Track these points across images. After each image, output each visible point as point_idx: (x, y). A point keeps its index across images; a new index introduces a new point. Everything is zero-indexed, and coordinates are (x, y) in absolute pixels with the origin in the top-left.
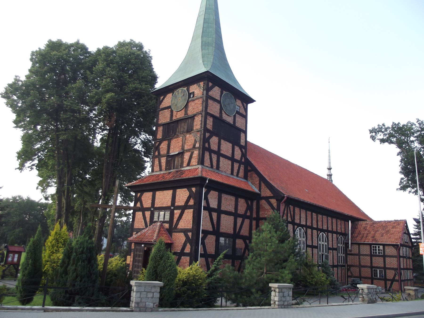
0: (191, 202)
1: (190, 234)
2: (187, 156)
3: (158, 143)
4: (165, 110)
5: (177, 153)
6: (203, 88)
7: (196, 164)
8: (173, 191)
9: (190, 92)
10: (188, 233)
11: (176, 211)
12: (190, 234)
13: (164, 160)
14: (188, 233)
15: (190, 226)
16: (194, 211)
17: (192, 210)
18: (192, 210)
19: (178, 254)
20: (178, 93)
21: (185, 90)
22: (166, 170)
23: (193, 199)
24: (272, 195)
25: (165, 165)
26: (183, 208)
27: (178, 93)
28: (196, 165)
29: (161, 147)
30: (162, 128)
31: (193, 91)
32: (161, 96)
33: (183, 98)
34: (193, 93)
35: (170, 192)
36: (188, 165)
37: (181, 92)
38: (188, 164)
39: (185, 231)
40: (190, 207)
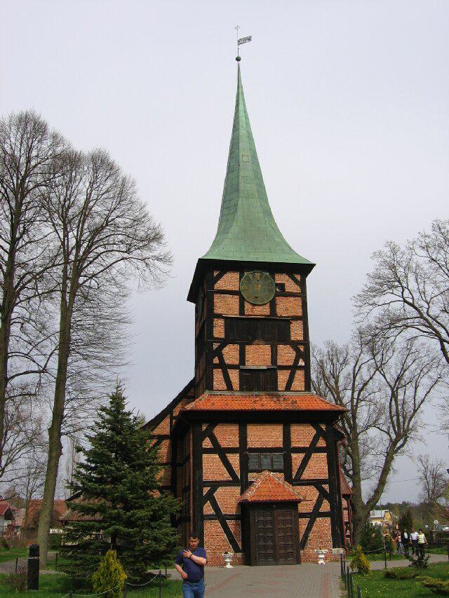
2: (283, 377)
4: (228, 295)
11: (294, 456)
12: (326, 487)
13: (234, 376)
15: (326, 476)
16: (328, 456)
17: (326, 454)
19: (310, 516)
22: (241, 389)
25: (238, 383)
26: (308, 452)
29: (223, 351)
30: (223, 322)
32: (217, 270)
34: (282, 286)
36: (288, 388)
39: (317, 483)
40: (321, 450)
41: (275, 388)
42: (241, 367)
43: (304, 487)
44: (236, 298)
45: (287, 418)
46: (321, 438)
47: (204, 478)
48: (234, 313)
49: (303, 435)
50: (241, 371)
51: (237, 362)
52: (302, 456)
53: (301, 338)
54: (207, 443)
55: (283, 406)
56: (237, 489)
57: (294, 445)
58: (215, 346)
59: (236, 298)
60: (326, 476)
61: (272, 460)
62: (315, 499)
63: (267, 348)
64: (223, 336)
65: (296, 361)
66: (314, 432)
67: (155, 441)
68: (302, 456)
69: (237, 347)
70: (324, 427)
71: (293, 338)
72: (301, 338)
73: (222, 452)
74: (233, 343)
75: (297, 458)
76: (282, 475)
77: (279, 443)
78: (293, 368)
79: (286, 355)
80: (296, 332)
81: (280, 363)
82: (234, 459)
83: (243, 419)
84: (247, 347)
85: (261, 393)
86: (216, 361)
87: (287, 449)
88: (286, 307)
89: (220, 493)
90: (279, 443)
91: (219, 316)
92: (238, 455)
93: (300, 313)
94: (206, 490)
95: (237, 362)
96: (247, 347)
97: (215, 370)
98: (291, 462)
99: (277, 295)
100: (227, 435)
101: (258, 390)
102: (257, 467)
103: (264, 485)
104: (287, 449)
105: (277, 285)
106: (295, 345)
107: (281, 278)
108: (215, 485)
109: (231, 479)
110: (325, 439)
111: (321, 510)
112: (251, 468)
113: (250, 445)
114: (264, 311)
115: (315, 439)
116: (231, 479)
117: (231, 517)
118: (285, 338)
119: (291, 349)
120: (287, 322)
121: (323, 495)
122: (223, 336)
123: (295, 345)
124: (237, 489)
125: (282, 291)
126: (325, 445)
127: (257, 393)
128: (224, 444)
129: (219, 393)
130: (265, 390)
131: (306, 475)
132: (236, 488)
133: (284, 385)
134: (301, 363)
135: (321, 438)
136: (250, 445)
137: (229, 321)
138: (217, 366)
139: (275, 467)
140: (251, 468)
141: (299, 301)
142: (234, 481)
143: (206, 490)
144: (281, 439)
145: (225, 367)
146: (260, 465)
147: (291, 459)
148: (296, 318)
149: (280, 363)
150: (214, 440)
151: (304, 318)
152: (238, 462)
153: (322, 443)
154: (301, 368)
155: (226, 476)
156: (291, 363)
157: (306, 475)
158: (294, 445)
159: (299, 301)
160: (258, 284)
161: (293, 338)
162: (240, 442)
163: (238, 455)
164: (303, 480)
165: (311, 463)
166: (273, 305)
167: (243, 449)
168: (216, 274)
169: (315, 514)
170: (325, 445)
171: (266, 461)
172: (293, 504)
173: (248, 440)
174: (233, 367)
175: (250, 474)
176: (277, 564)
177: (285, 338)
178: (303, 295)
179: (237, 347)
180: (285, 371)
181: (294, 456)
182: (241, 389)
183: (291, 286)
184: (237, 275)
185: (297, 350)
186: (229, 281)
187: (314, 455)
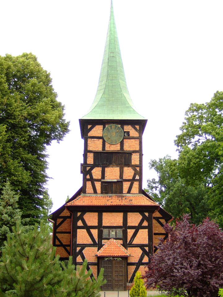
0: (145, 224)
1: (147, 249)
2: (126, 185)
3: (89, 168)
5: (116, 180)
6: (139, 131)
7: (138, 193)
8: (123, 214)
9: (125, 130)
10: (145, 248)
11: (129, 230)
12: (147, 249)
13: (98, 185)
14: (145, 248)
15: (146, 242)
17: (147, 230)
18: (147, 230)
19: (136, 264)
20: (111, 128)
21: (118, 127)
22: (102, 193)
23: (147, 221)
24: (161, 216)
26: (137, 229)
27: (111, 128)
28: (137, 194)
29: (92, 171)
31: (128, 130)
32: (90, 125)
33: (117, 134)
35: (121, 215)
36: (129, 192)
37: (115, 128)
38: (129, 192)
39: (142, 246)
40: (144, 228)
41: (121, 191)
42: (103, 180)
43: (133, 248)
44: (101, 140)
45: (125, 210)
46: (145, 221)
47: (78, 243)
48: (99, 148)
49: (134, 219)
50: (102, 183)
51: (100, 178)
52: (134, 230)
53: (138, 163)
54: (80, 223)
55: (124, 203)
56: (96, 249)
57: (129, 224)
58: (88, 168)
59: (101, 140)
60: (146, 242)
61: (116, 233)
62: (140, 255)
63: (117, 169)
64: (92, 163)
65: (134, 177)
66: (141, 217)
67: (61, 220)
68: (134, 230)
69: (100, 169)
70: (147, 214)
71: (133, 163)
72: (138, 163)
73: (88, 228)
74: (98, 167)
75: (130, 232)
76: (121, 242)
77: (121, 224)
78: (133, 180)
79: (128, 173)
80: (135, 159)
81: (124, 178)
82: (95, 232)
83: (100, 210)
84: (106, 169)
85: (114, 195)
86: (88, 177)
87: (125, 227)
88: (129, 146)
89: (86, 251)
90: (121, 224)
91: (91, 152)
92: (97, 230)
93: (138, 149)
94: (78, 249)
95: (100, 178)
96: (106, 169)
97: (87, 182)
98: (127, 234)
99: (124, 139)
100: (91, 219)
101: (112, 193)
102: (107, 237)
103: (109, 247)
104: (125, 227)
105: (125, 132)
106: (134, 167)
107: (127, 128)
108: (83, 246)
109: (92, 243)
110: (147, 221)
111: (143, 261)
112: (104, 237)
113: (104, 225)
114: (117, 148)
115: (142, 221)
116: (92, 243)
117: (93, 264)
118: (128, 163)
119: (132, 170)
120: (130, 154)
121: (145, 253)
122: (92, 163)
123: (134, 167)
124: (96, 249)
125: (127, 136)
126: (147, 225)
127: (111, 195)
128: (89, 224)
129: (89, 195)
130: (116, 193)
131: (135, 242)
132: (95, 248)
133: (127, 190)
134: (137, 177)
135: (145, 221)
136: (104, 225)
137: (96, 154)
138: (88, 180)
139: (118, 237)
140: (104, 237)
141: (137, 142)
142: (94, 244)
143: (78, 249)
144: (122, 221)
145: (92, 180)
146: (109, 235)
147: (127, 232)
148: (135, 152)
149: (124, 178)
150: (84, 222)
151: (140, 152)
152: (97, 233)
153: (145, 224)
154: (137, 180)
155: (90, 241)
156: (131, 178)
157: (135, 242)
158: (129, 224)
159: (137, 142)
160: (114, 132)
161: (133, 163)
162: (98, 223)
163: (97, 230)
164: (134, 244)
165: (138, 235)
166: (122, 144)
167: (100, 227)
168: (89, 127)
169: (140, 263)
170: (147, 225)
171: (113, 233)
172: (125, 258)
173: (103, 221)
174: (98, 180)
175: (103, 241)
176: (113, 291)
177: (128, 163)
178: (140, 139)
179: (100, 169)
180: (127, 183)
181: (129, 230)
182: (102, 193)
183: (133, 133)
184: (101, 127)
185: (135, 170)
186: (97, 131)
187: (141, 231)
